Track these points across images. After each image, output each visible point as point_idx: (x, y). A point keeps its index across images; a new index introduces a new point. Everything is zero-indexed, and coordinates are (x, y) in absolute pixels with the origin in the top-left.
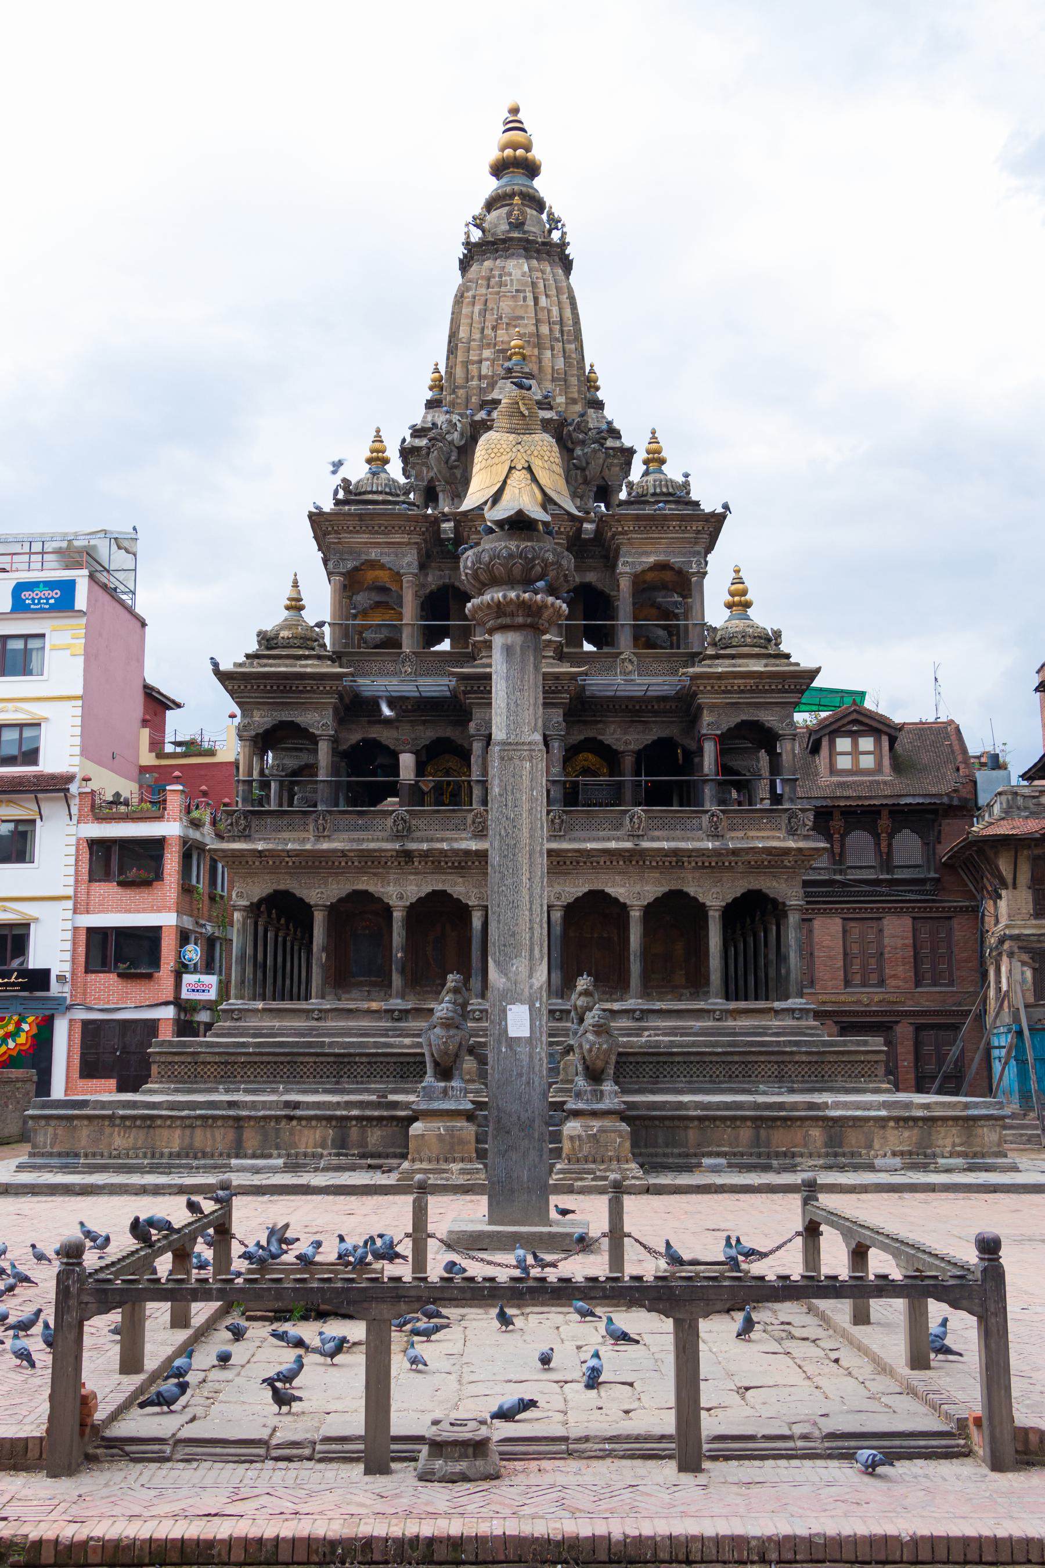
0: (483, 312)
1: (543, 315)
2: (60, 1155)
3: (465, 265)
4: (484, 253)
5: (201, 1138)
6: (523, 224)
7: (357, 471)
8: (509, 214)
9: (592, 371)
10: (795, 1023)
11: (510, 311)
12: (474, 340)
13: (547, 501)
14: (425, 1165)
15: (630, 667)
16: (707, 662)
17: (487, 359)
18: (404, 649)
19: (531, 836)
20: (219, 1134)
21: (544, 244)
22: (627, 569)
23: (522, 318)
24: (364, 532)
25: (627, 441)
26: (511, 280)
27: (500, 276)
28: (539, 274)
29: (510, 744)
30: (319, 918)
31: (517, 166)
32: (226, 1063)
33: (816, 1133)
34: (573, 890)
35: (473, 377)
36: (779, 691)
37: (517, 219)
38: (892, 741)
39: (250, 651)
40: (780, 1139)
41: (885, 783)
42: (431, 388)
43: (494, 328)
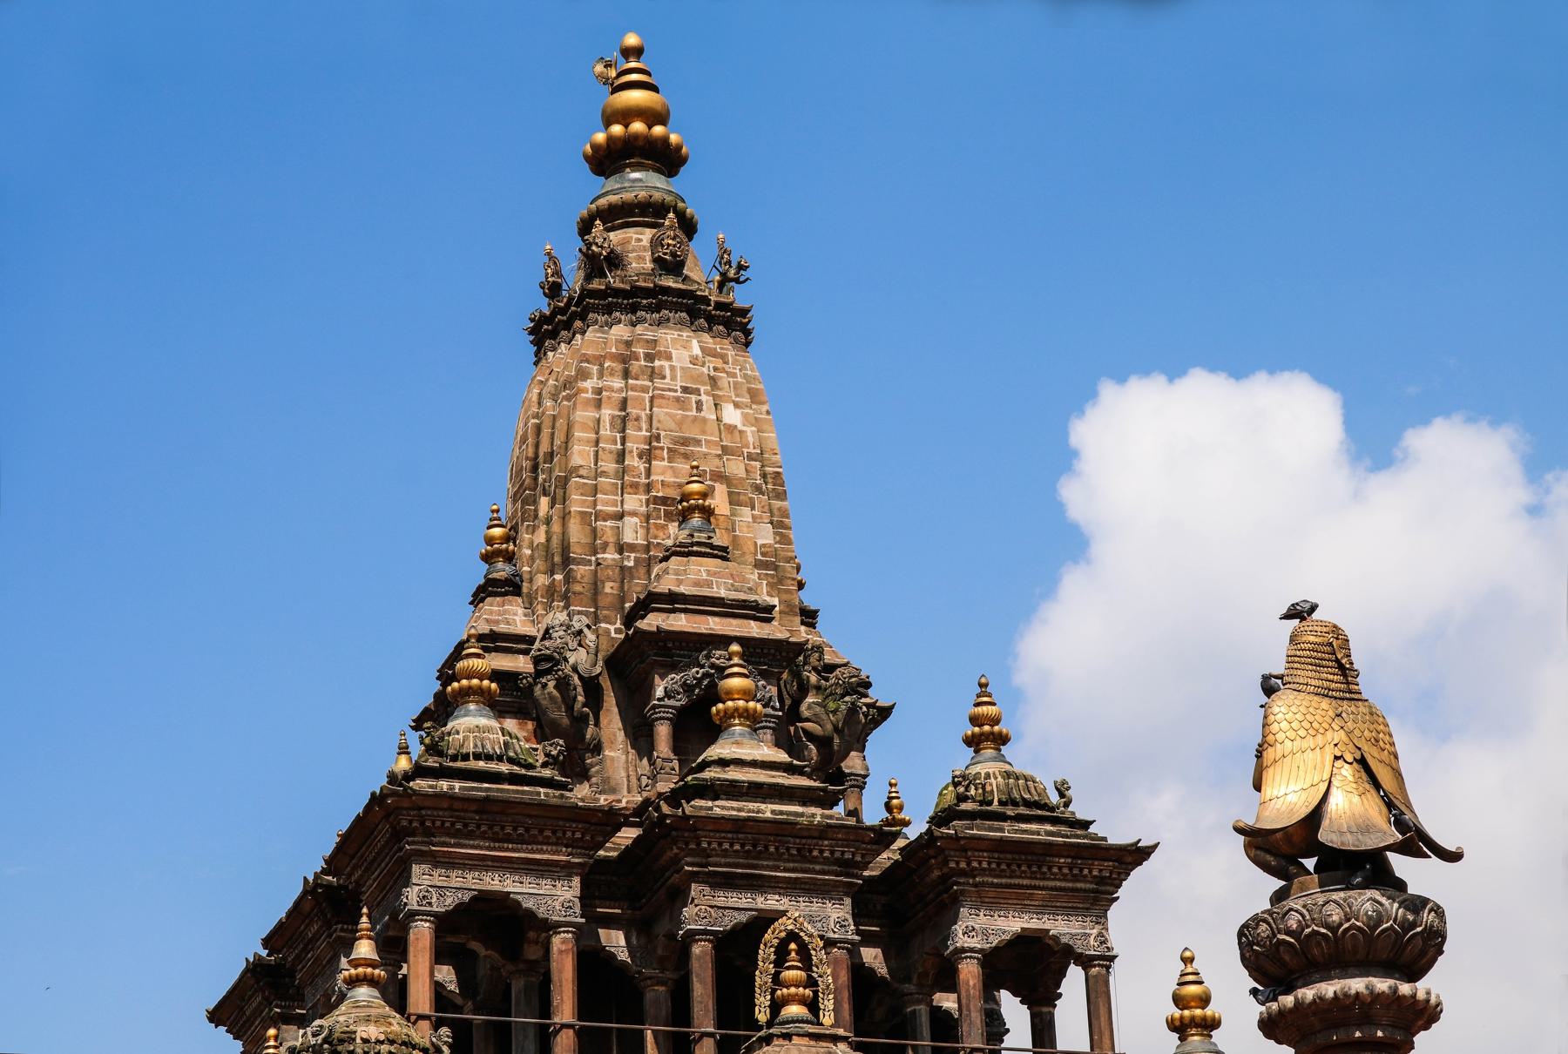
0: (622, 423)
4: (608, 310)
6: (682, 264)
8: (656, 243)
11: (673, 426)
12: (603, 474)
17: (634, 514)
21: (719, 306)
22: (974, 943)
23: (698, 442)
24: (483, 837)
26: (672, 368)
27: (650, 358)
28: (720, 364)
35: (606, 545)
43: (648, 456)
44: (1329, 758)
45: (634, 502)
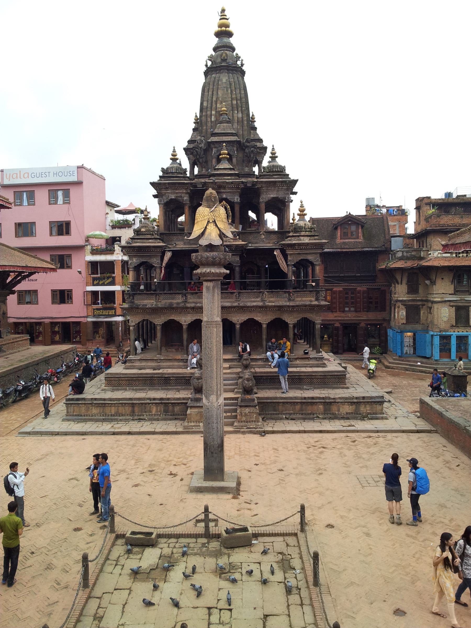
1: (234, 96)
2: (76, 415)
3: (206, 74)
4: (212, 71)
5: (121, 410)
6: (226, 59)
7: (167, 164)
9: (253, 115)
10: (317, 362)
13: (222, 235)
14: (192, 424)
15: (263, 237)
16: (289, 238)
18: (186, 232)
19: (217, 354)
20: (127, 408)
25: (265, 144)
29: (209, 322)
30: (159, 328)
31: (224, 33)
32: (129, 380)
33: (321, 407)
34: (243, 318)
36: (315, 249)
37: (224, 58)
38: (362, 227)
39: (131, 237)
40: (309, 409)
41: (359, 242)
42: (194, 123)
44: (207, 222)
45: (213, 112)
